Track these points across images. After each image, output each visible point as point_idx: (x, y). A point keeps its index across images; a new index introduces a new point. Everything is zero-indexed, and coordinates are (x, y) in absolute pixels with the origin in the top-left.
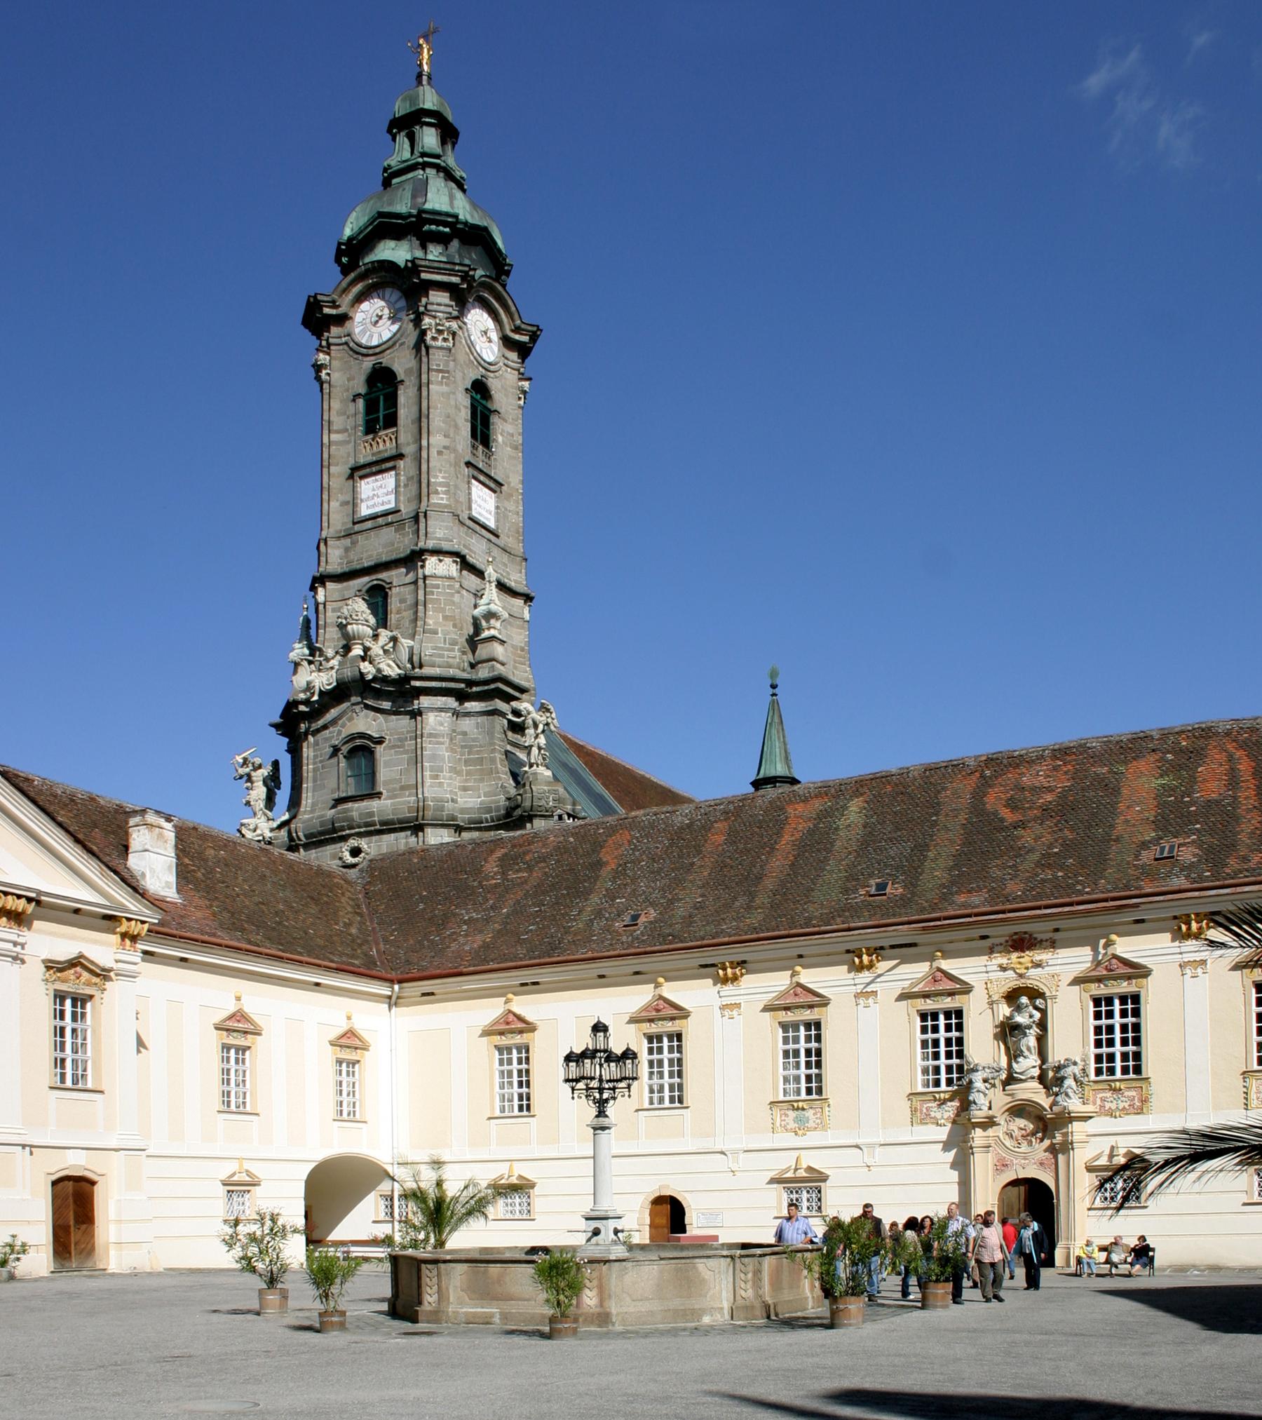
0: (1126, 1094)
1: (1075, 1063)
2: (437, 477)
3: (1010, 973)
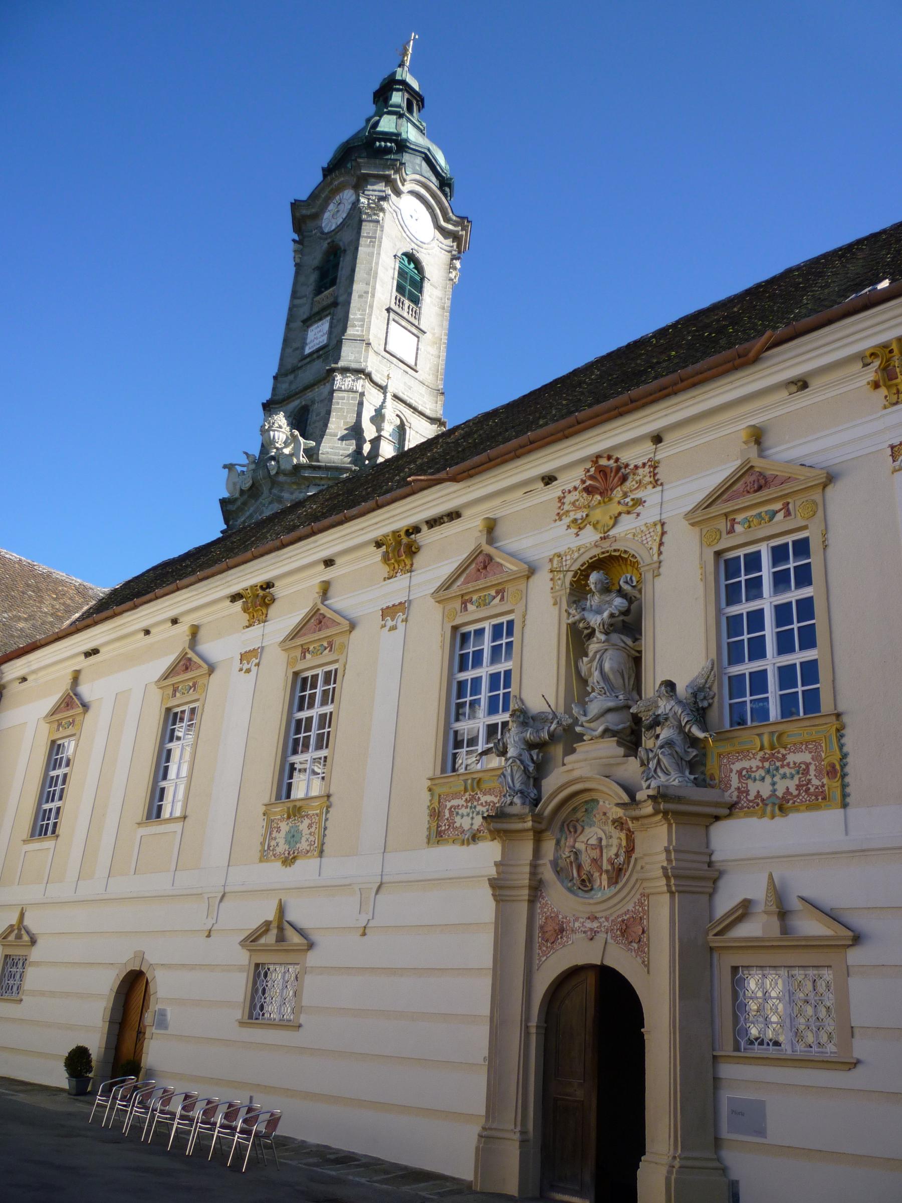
2: (355, 314)
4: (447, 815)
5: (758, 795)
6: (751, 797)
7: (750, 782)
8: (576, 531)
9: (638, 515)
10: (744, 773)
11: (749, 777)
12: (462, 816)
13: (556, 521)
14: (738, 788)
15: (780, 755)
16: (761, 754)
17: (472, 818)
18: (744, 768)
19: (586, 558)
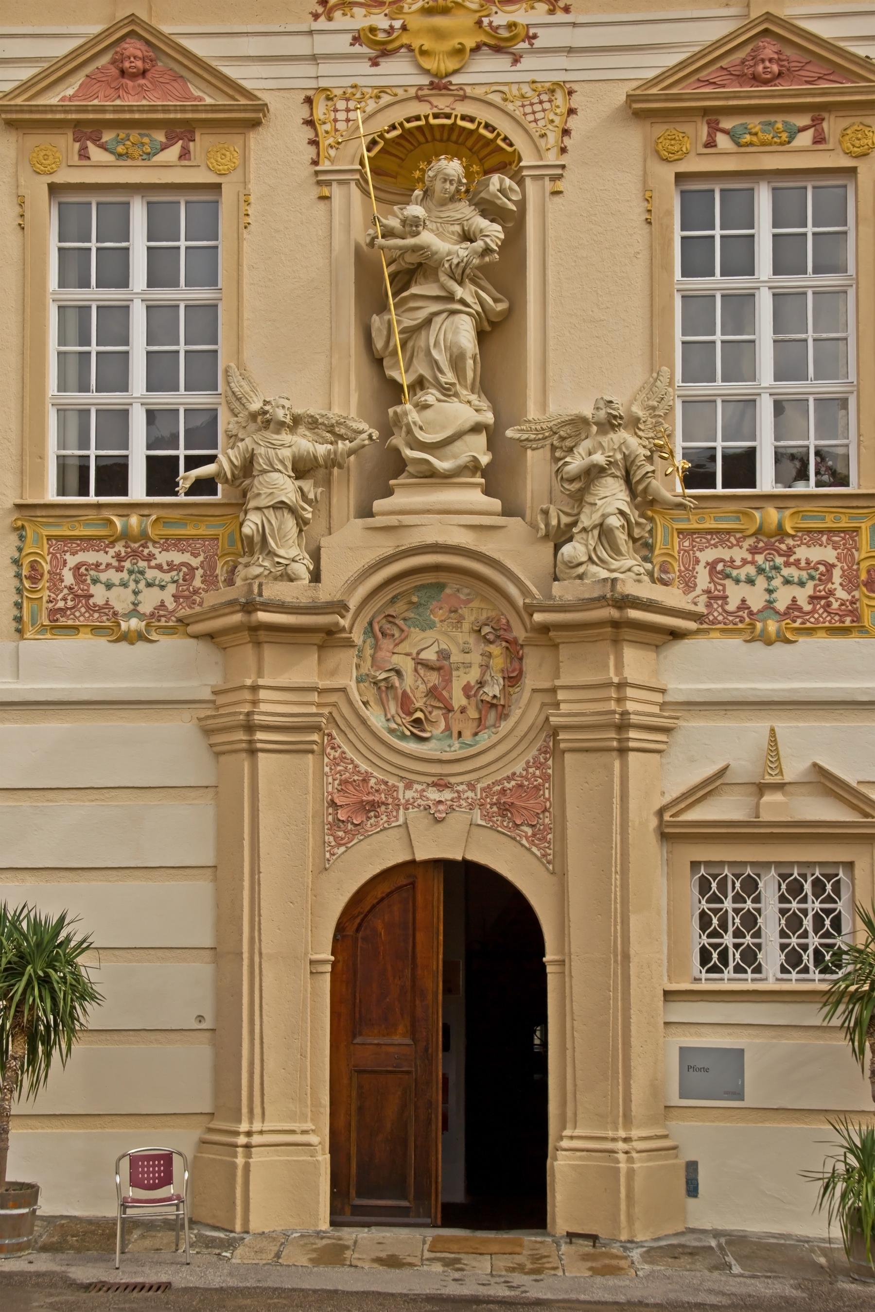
0: (802, 553)
1: (634, 423)
3: (399, 72)
4: (68, 578)
5: (743, 605)
6: (732, 606)
7: (728, 583)
8: (372, 53)
9: (516, 61)
10: (720, 567)
11: (728, 576)
12: (109, 586)
13: (316, 16)
14: (708, 591)
15: (783, 547)
16: (751, 541)
17: (136, 593)
18: (722, 560)
19: (398, 115)
